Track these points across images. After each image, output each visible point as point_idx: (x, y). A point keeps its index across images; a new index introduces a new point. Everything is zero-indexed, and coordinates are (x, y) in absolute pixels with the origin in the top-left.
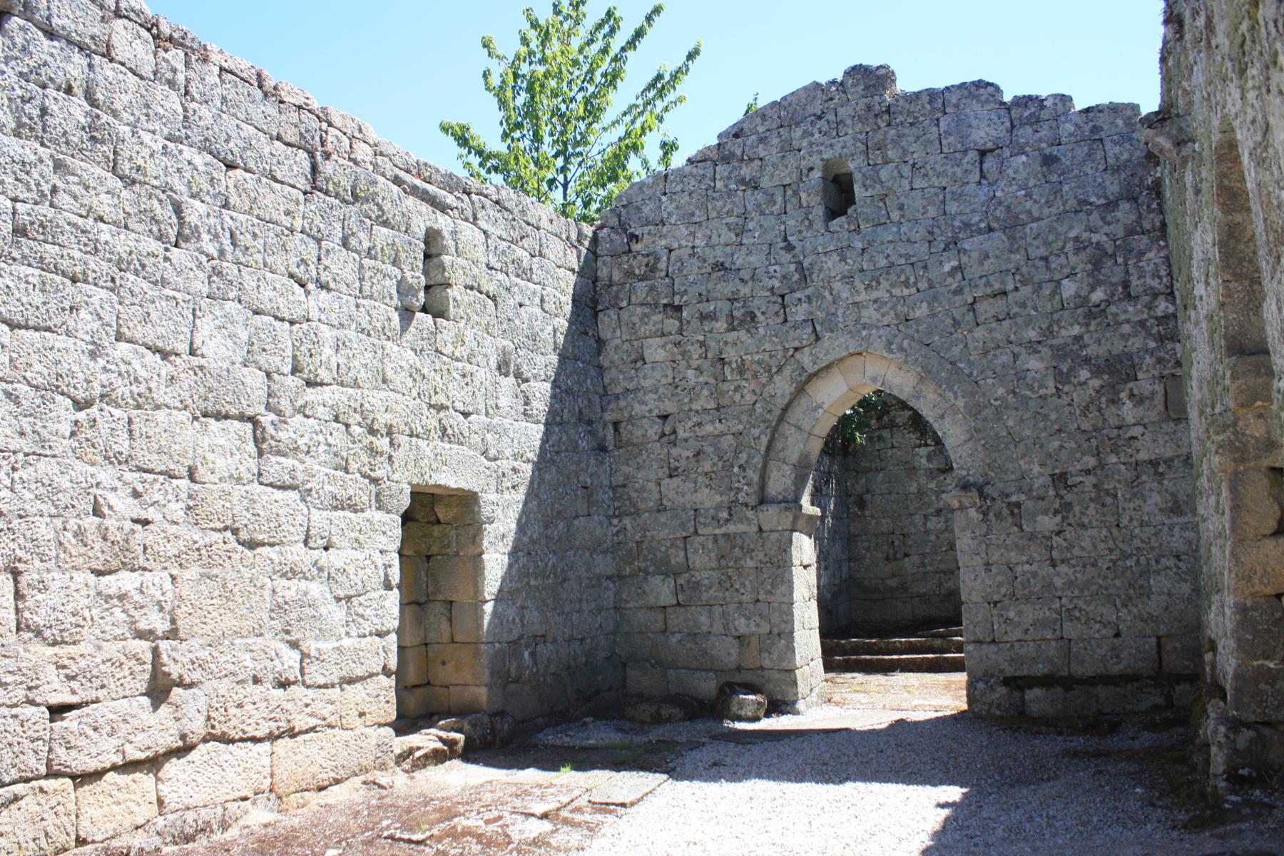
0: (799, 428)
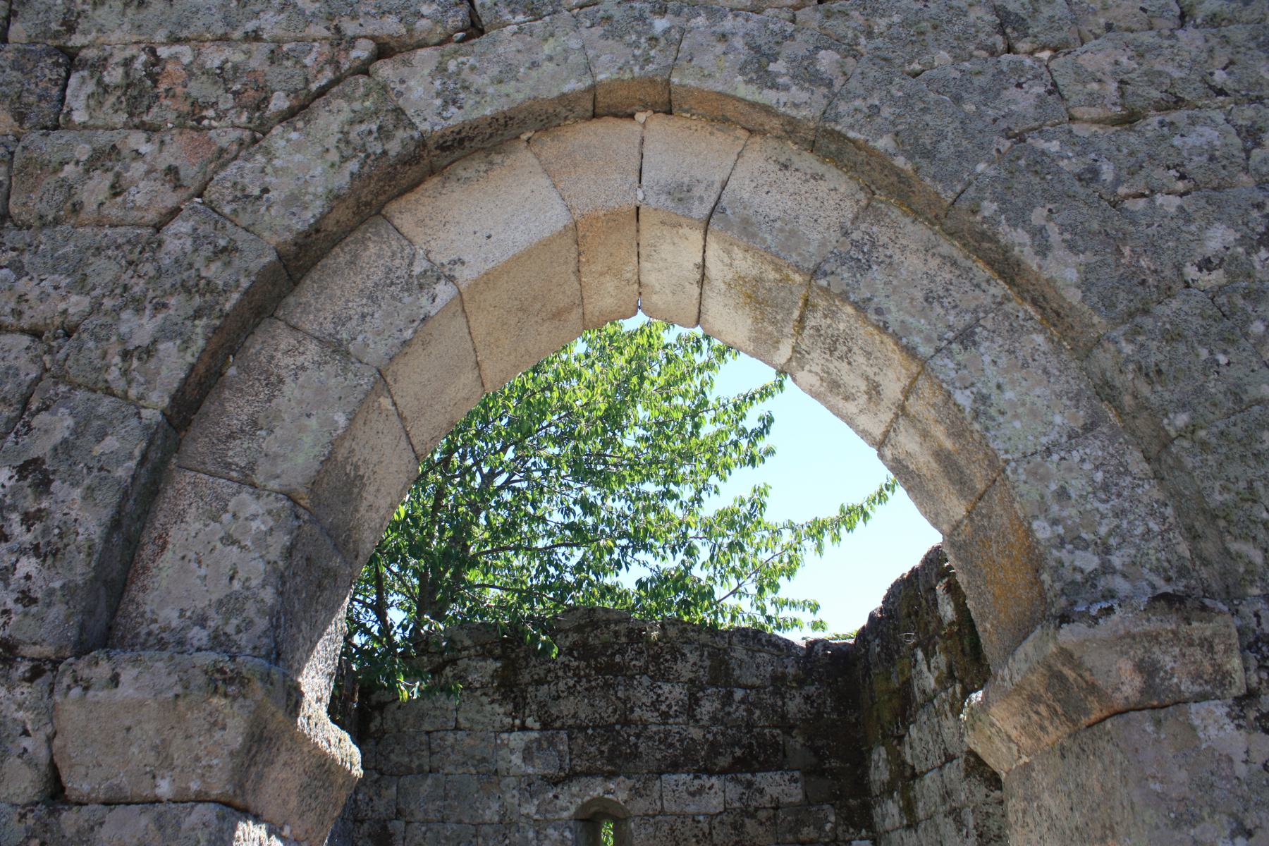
0: (336, 348)
